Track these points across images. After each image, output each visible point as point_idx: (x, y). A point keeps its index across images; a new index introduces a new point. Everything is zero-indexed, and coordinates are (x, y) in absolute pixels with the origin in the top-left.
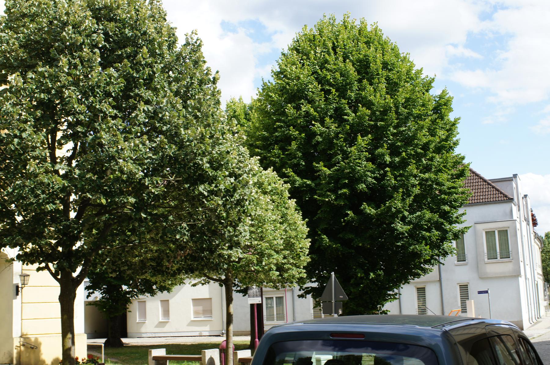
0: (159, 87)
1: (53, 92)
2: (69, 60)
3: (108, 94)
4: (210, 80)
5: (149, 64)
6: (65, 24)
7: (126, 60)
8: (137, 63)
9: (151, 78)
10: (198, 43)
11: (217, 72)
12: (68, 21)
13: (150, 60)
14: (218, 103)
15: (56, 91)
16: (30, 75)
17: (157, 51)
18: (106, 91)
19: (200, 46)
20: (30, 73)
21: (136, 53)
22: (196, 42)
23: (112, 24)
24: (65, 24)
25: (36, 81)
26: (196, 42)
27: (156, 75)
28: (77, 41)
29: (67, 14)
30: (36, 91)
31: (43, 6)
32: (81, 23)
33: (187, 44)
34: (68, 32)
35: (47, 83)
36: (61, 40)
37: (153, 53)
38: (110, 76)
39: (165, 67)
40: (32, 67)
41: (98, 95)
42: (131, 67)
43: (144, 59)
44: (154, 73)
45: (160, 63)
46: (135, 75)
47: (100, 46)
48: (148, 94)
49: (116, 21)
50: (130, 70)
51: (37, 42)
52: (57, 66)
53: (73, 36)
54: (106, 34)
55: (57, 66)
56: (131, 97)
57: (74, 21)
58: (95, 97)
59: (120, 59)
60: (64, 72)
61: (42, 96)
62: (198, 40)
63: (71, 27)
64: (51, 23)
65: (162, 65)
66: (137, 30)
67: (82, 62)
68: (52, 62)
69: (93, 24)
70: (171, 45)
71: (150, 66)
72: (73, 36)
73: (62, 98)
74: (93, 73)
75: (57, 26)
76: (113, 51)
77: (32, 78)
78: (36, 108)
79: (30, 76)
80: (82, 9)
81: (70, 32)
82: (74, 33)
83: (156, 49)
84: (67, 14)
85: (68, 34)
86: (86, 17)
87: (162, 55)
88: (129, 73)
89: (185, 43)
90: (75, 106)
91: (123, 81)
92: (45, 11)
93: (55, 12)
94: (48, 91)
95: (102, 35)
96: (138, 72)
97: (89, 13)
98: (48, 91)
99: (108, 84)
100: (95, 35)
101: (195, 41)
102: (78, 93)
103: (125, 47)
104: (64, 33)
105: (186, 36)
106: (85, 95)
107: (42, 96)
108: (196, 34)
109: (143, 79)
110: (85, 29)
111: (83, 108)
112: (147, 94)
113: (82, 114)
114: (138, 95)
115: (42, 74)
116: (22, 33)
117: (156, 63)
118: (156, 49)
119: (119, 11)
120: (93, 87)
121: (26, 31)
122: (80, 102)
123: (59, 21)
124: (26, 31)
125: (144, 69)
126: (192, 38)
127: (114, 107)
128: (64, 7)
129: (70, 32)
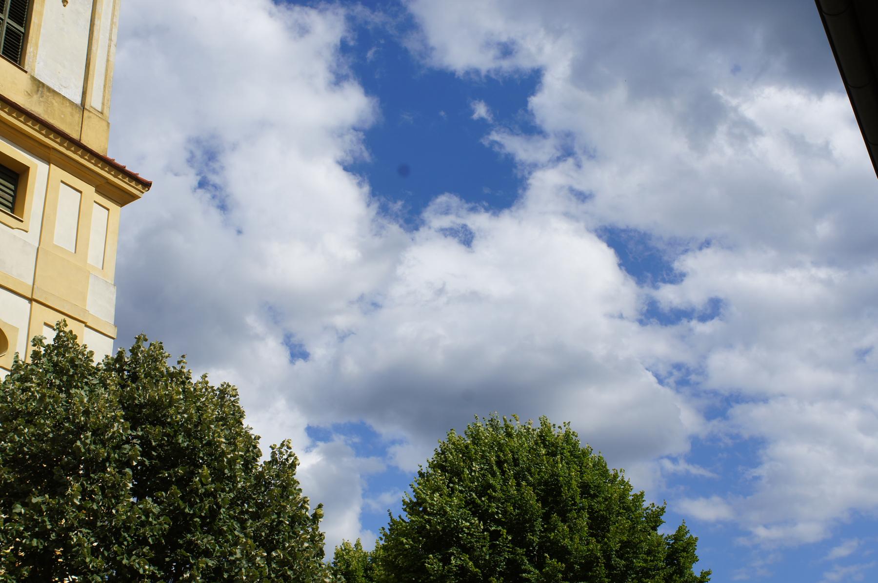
0: (225, 528)
1: (53, 536)
2: (82, 485)
3: (144, 542)
4: (308, 518)
5: (212, 492)
6: (82, 428)
7: (174, 487)
8: (191, 491)
9: (213, 514)
10: (290, 462)
11: (320, 506)
12: (86, 423)
13: (212, 487)
14: (321, 554)
15: (58, 535)
16: (19, 509)
17: (226, 471)
18: (139, 536)
19: (293, 466)
20: (19, 506)
21: (192, 474)
22: (287, 460)
23: (158, 429)
24: (82, 428)
25: (26, 519)
26: (287, 460)
27: (222, 510)
28: (98, 455)
29: (86, 413)
30: (26, 534)
31: (48, 400)
32: (108, 426)
33: (274, 461)
34: (85, 442)
35: (44, 521)
36: (73, 453)
37: (218, 476)
38: (147, 512)
39: (236, 498)
40: (23, 497)
41: (125, 543)
42: (182, 498)
43: (203, 485)
44: (219, 507)
45: (231, 491)
46: (187, 510)
47: (135, 463)
48: (205, 541)
49: (164, 424)
50: (181, 502)
51: (33, 456)
52: (63, 496)
53: (92, 447)
54: (145, 442)
55: (63, 496)
56: (181, 546)
57: (95, 423)
58: (120, 544)
59: (165, 485)
60: (74, 504)
61: (35, 542)
62: (290, 456)
63: (89, 434)
64: (58, 426)
65: (232, 495)
66: (196, 438)
67: (102, 489)
68: (56, 488)
69: (125, 430)
70: (249, 463)
71: (213, 495)
72: (92, 447)
73: (68, 548)
74: (120, 507)
75: (69, 432)
76: (153, 471)
77: (20, 514)
78: (25, 561)
79: (17, 511)
80: (110, 406)
81: (88, 441)
82: (95, 443)
83: (225, 467)
84: (86, 413)
85: (84, 444)
86: (115, 418)
87: (232, 479)
88: (178, 507)
89: (269, 459)
90: (88, 560)
91: (168, 519)
92: (50, 407)
93: (66, 410)
94: (43, 535)
95: (137, 446)
96: (191, 506)
97: (120, 413)
98: (43, 535)
99: (143, 524)
100: (127, 446)
101: (285, 457)
102: (93, 539)
103: (175, 465)
104: (78, 443)
105: (273, 449)
106: (105, 542)
107: (35, 542)
108: (289, 448)
109: (200, 517)
110: (112, 437)
111: (99, 562)
112: (205, 540)
113: (97, 574)
114: (190, 542)
115: (37, 508)
116: (11, 442)
117: (223, 490)
118: (225, 467)
119: (172, 411)
120: (118, 530)
121: (17, 439)
122: (95, 552)
123: (73, 423)
124: (17, 439)
125: (202, 501)
126: (281, 453)
127: (151, 562)
128: (82, 402)
129: (88, 441)
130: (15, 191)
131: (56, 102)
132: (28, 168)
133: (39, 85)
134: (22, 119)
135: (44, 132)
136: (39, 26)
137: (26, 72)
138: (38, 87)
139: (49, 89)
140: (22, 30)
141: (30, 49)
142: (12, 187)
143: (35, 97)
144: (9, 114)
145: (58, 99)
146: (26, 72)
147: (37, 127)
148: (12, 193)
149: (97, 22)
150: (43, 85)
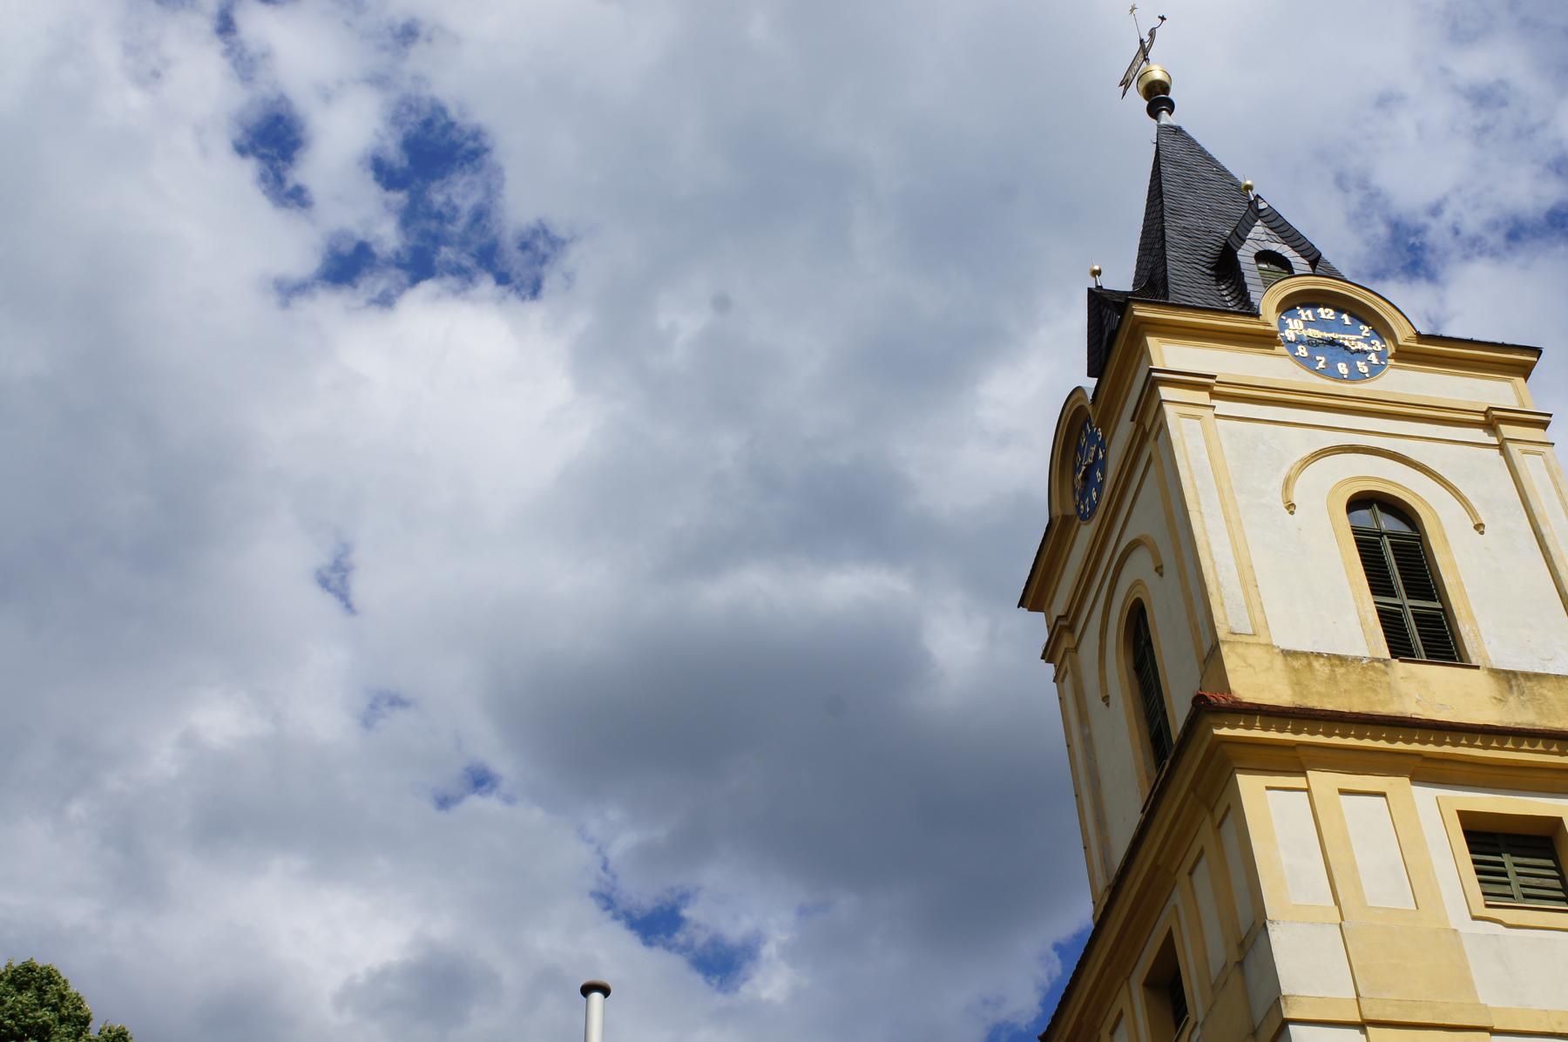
130: (1558, 868)
131: (1547, 691)
132: (1560, 820)
133: (1508, 678)
134: (1509, 745)
135: (1555, 749)
136: (1460, 585)
137: (1477, 667)
138: (1509, 681)
139: (1528, 676)
140: (1438, 605)
141: (1464, 628)
142: (1550, 863)
143: (1512, 699)
144: (1486, 747)
145: (1549, 685)
146: (1477, 667)
147: (1540, 747)
148: (1554, 873)
149: (1545, 530)
150: (1514, 673)
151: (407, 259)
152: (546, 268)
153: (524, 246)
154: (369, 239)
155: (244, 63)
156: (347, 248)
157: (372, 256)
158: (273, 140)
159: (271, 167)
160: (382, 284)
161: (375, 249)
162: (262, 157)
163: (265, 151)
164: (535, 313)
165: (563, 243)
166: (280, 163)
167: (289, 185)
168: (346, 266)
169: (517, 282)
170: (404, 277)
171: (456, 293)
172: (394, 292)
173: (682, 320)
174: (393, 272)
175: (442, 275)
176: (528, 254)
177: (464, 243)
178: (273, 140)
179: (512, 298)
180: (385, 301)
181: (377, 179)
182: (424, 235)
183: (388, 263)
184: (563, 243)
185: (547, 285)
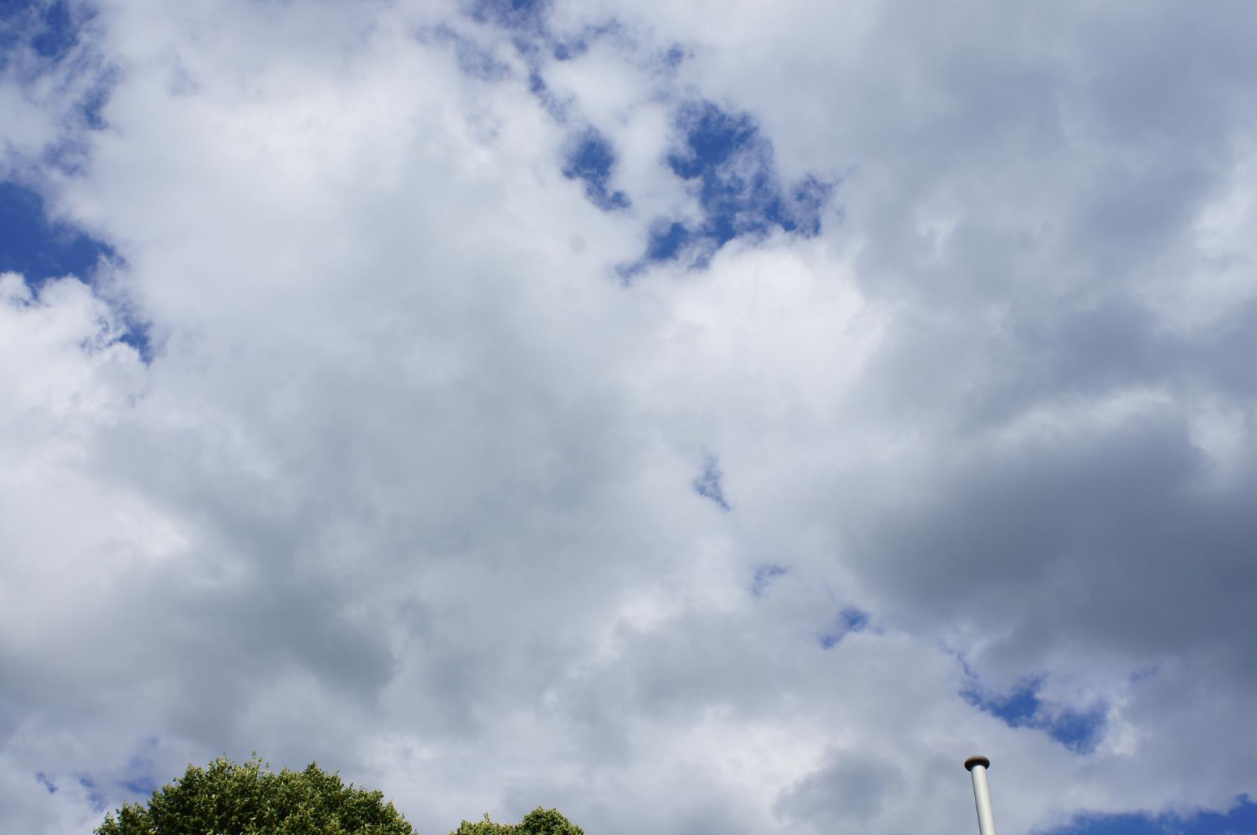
151: (712, 228)
152: (820, 210)
153: (801, 197)
154: (680, 220)
155: (558, 110)
156: (665, 230)
157: (685, 232)
158: (591, 161)
159: (595, 182)
160: (697, 252)
161: (686, 226)
162: (586, 176)
163: (587, 172)
164: (819, 246)
165: (830, 187)
166: (601, 178)
167: (610, 194)
168: (667, 244)
169: (801, 225)
170: (712, 242)
171: (755, 245)
172: (707, 256)
173: (937, 225)
174: (704, 240)
175: (741, 234)
176: (805, 202)
177: (753, 205)
178: (591, 161)
179: (799, 239)
180: (702, 264)
181: (676, 172)
182: (722, 206)
183: (698, 235)
184: (830, 187)
185: (824, 222)
